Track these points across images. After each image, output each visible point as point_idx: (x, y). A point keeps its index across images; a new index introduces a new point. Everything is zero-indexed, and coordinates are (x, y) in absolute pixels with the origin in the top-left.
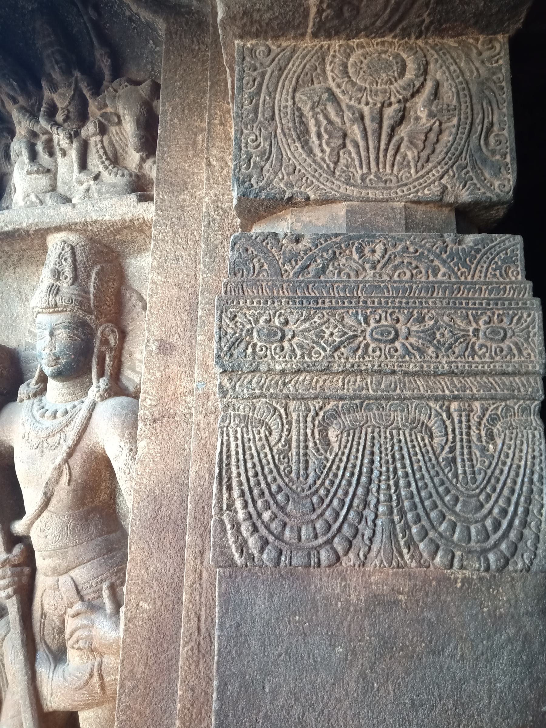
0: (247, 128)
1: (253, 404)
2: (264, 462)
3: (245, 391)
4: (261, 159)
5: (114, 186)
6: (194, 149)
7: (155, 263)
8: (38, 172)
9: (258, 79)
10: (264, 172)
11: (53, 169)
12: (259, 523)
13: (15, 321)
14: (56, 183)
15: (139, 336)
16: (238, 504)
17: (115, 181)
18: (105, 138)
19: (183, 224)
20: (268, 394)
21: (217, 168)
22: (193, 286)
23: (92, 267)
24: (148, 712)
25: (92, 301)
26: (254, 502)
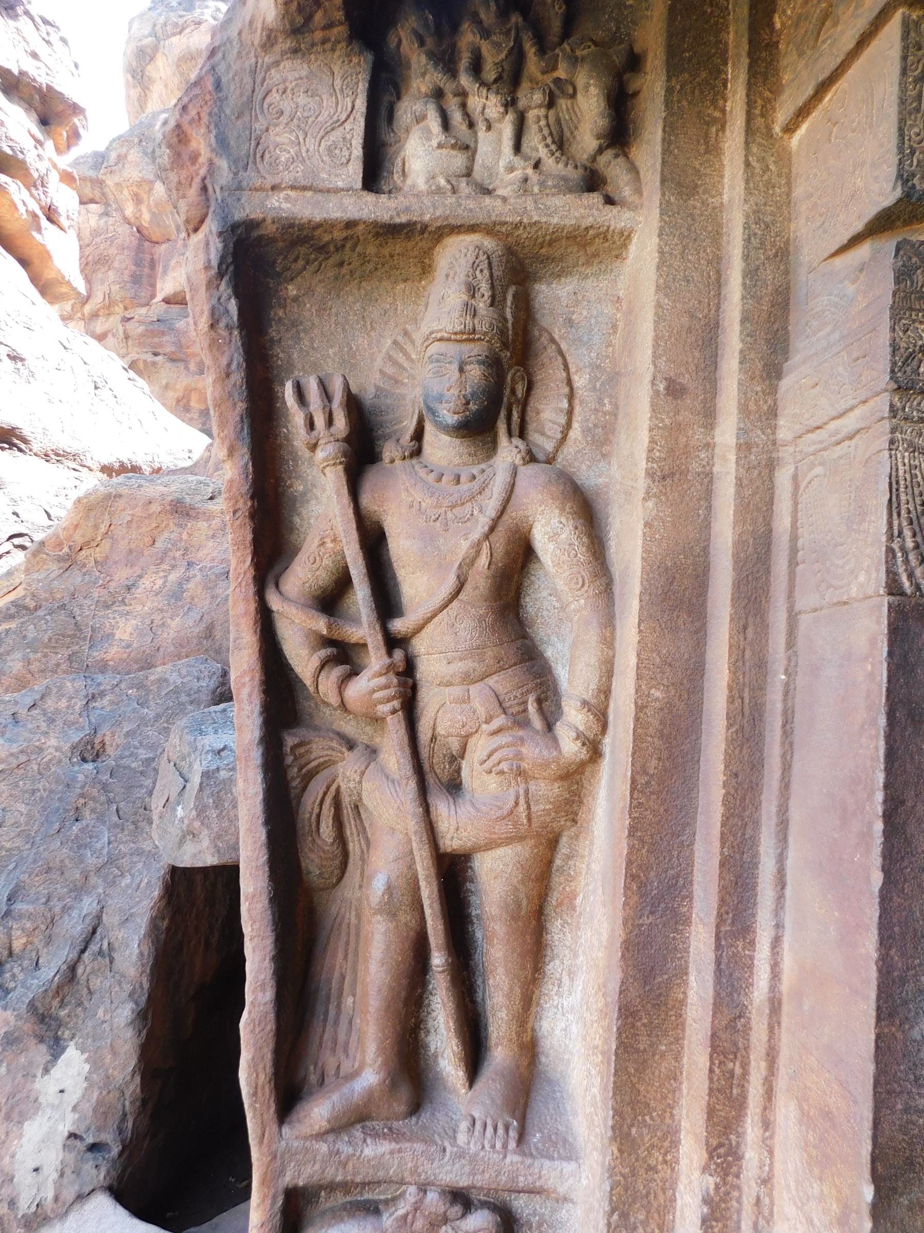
3: (915, 413)
5: (565, 179)
6: (707, 143)
7: (661, 281)
8: (453, 147)
11: (472, 145)
13: (354, 357)
14: (473, 166)
16: (907, 533)
18: (552, 113)
21: (758, 170)
23: (508, 287)
24: (662, 810)
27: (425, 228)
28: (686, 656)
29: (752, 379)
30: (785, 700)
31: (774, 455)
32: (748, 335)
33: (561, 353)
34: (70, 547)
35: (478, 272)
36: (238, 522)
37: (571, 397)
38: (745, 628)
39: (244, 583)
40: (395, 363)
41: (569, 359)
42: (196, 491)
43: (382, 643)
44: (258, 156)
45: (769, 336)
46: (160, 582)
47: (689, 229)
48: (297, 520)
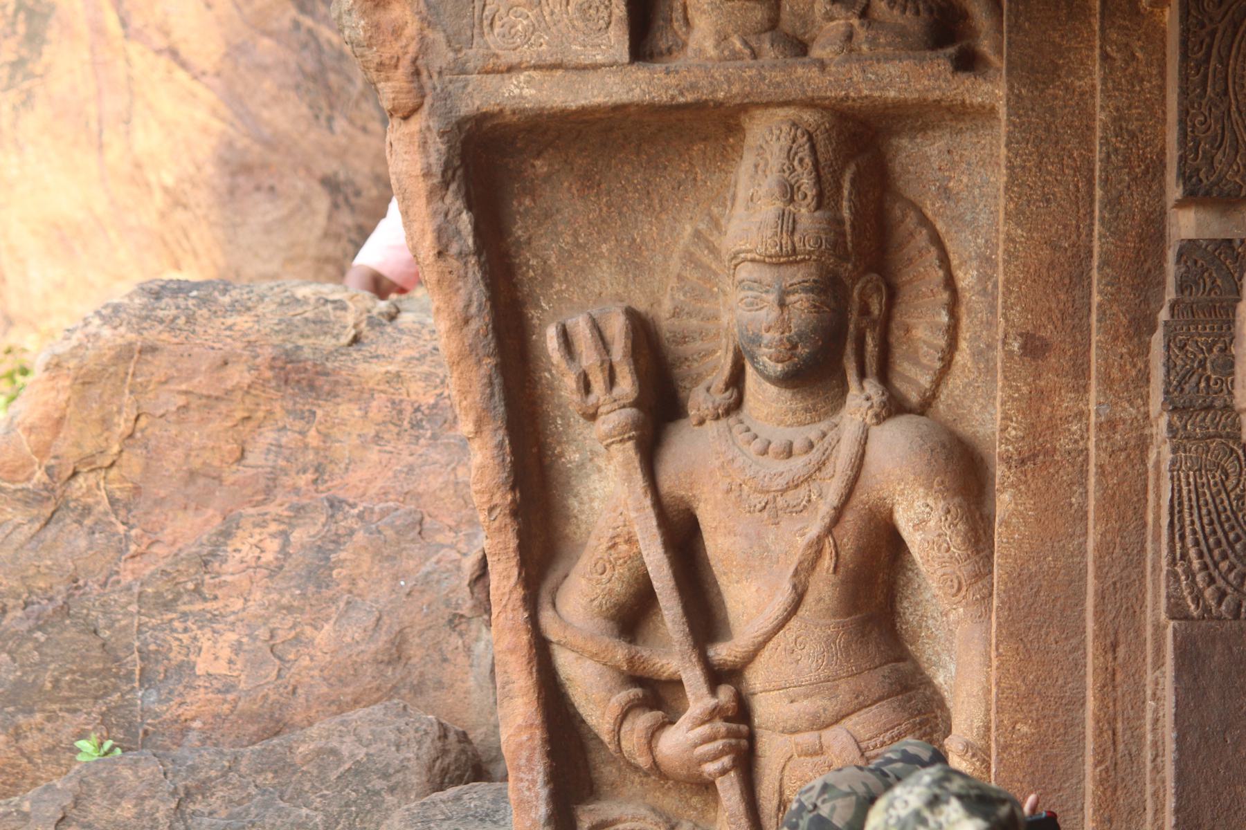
0: (1193, 108)
1: (1207, 446)
2: (1220, 508)
4: (1212, 146)
5: (902, 33)
7: (1012, 206)
9: (1208, 40)
10: (1216, 164)
12: (1216, 574)
14: (778, 15)
15: (925, 295)
16: (1192, 553)
17: (900, 21)
19: (1054, 139)
20: (1224, 433)
22: (1074, 245)
23: (843, 169)
25: (849, 238)
26: (1210, 551)
27: (719, 105)
28: (1060, 682)
29: (1115, 339)
30: (1154, 730)
31: (1147, 431)
32: (1106, 285)
33: (937, 240)
34: (49, 471)
35: (796, 163)
36: (496, 524)
37: (953, 307)
38: (1114, 646)
39: (510, 607)
40: (698, 265)
41: (949, 245)
42: (321, 324)
43: (702, 680)
44: (486, 23)
45: (1137, 281)
46: (273, 546)
47: (1048, 130)
48: (574, 503)
